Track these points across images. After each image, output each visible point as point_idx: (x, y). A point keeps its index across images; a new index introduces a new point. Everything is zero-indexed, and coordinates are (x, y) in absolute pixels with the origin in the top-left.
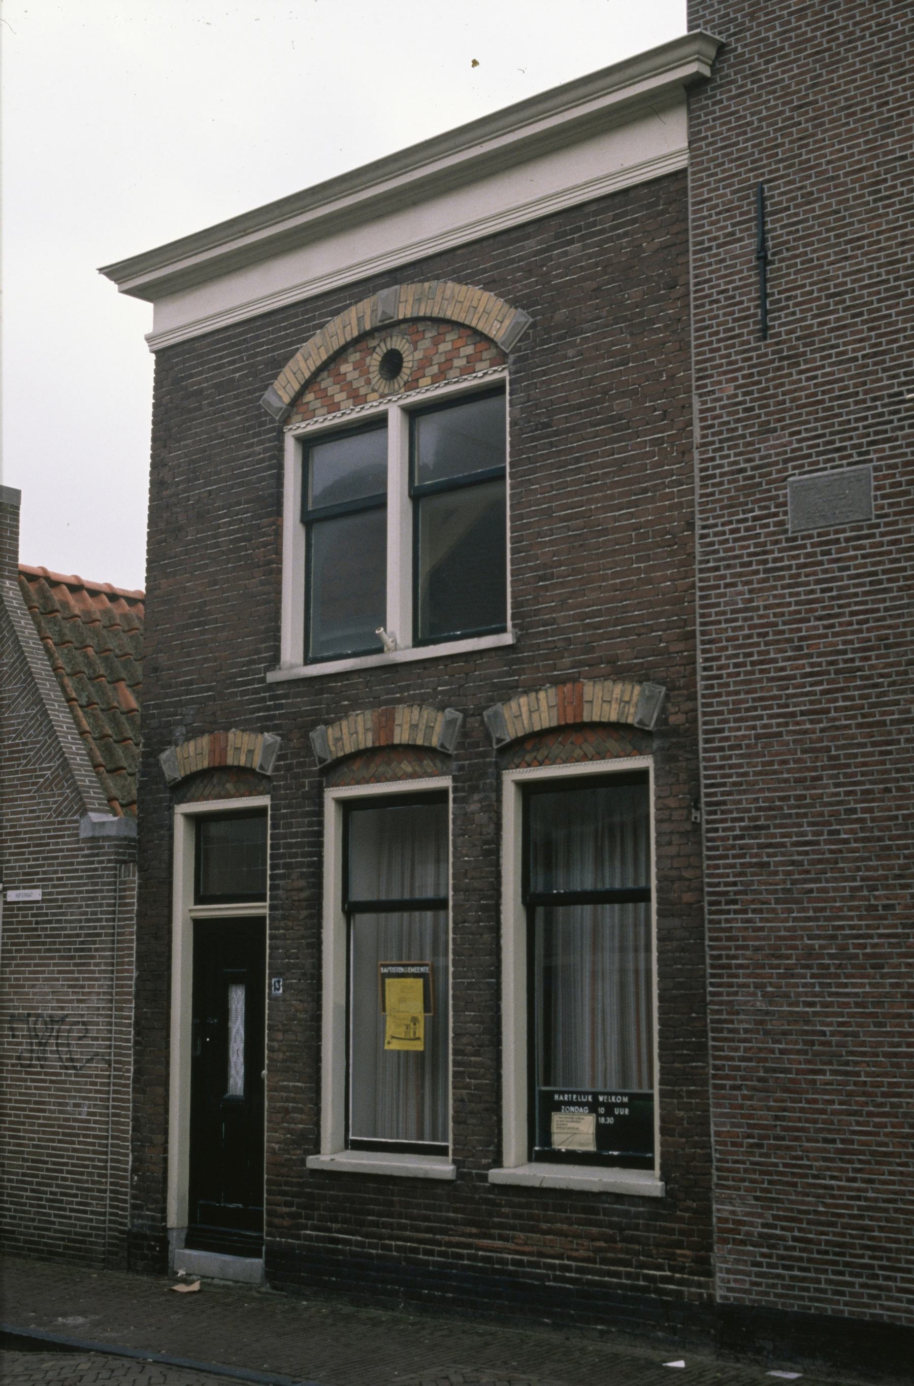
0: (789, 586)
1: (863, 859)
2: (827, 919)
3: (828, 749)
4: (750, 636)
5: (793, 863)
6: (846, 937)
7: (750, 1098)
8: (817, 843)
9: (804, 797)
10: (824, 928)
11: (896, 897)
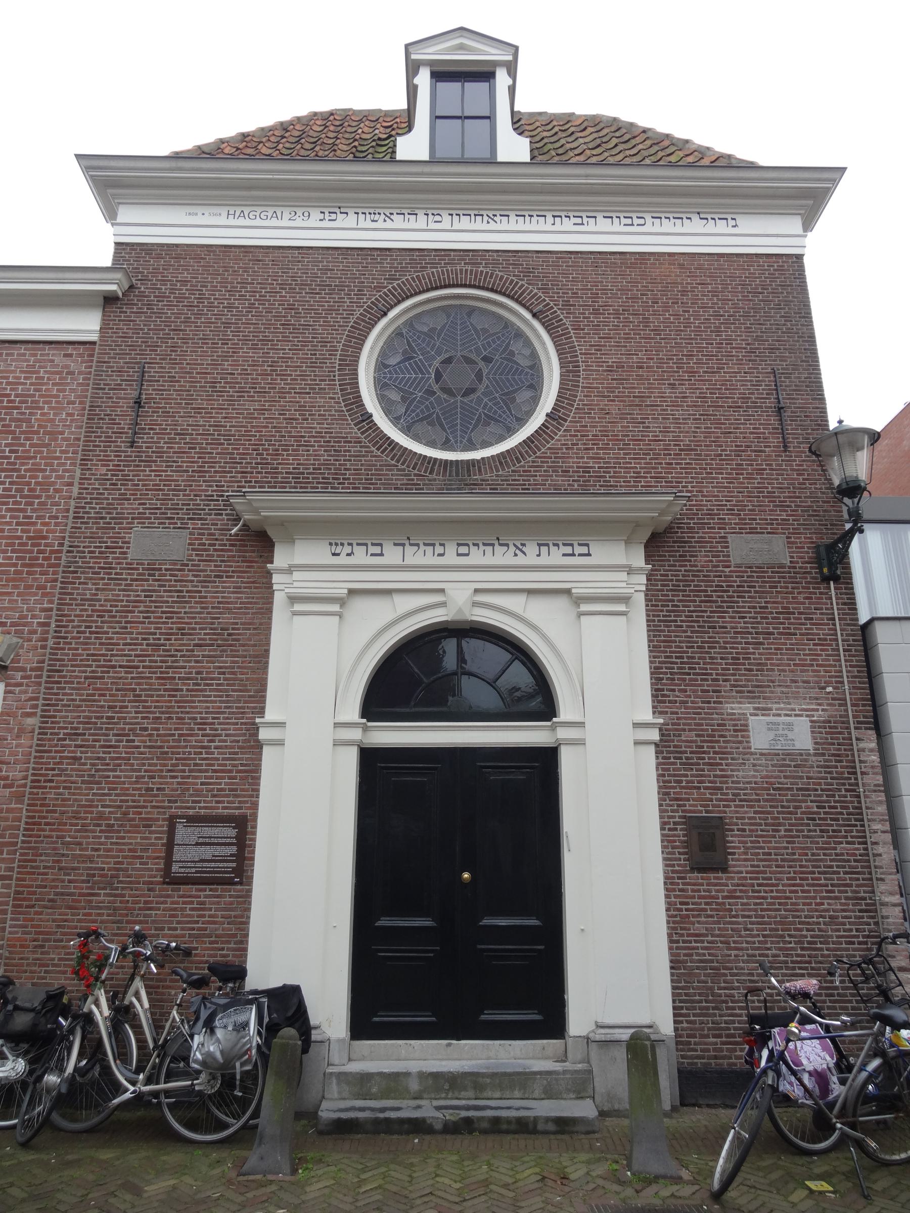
0: (124, 590)
1: (148, 759)
2: (116, 795)
3: (134, 690)
4: (91, 616)
5: (98, 758)
6: (128, 807)
7: (41, 913)
8: (118, 747)
9: (113, 718)
10: (115, 801)
11: (167, 783)
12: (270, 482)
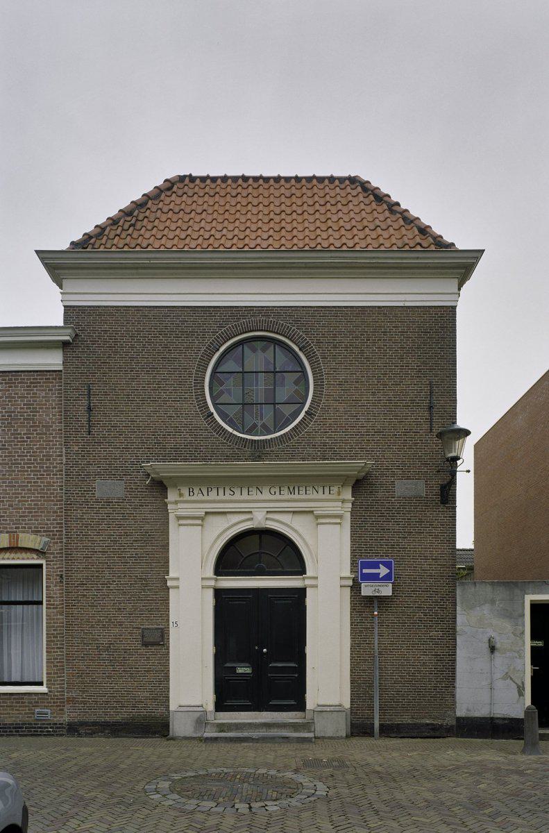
12: (162, 454)
